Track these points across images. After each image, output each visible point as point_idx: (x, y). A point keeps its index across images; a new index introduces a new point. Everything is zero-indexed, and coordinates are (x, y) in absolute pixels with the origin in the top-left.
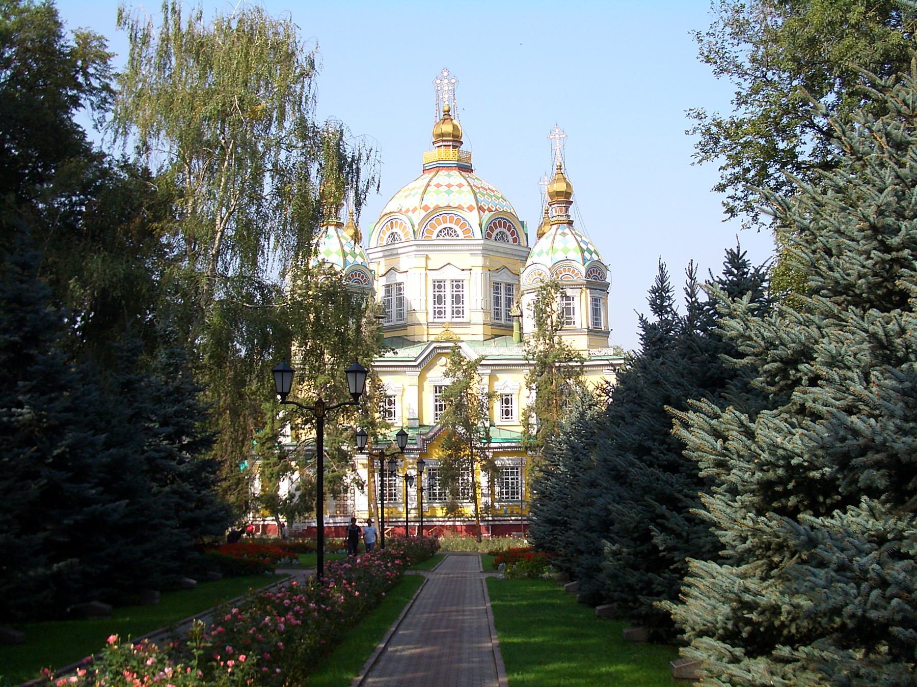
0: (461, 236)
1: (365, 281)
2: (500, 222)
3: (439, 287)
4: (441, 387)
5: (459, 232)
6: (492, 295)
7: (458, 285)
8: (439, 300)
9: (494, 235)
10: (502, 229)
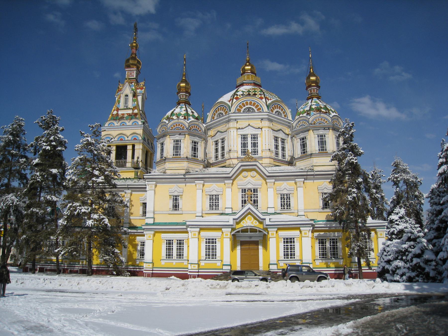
0: (256, 111)
1: (200, 131)
4: (245, 190)
5: (256, 110)
6: (274, 143)
7: (254, 137)
8: (244, 145)
9: (274, 112)
10: (278, 110)
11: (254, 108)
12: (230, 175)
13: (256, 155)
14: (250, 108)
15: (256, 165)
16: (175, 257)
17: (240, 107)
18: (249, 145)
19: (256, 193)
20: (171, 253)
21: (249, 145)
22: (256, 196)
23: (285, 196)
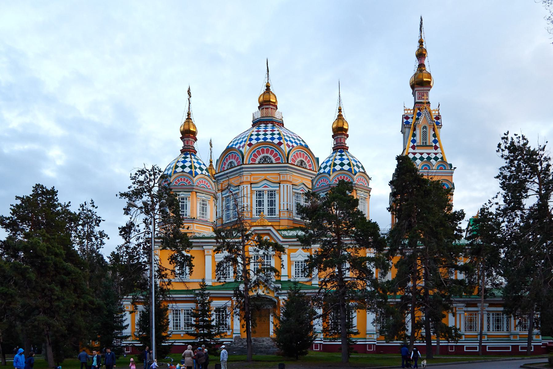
2: (300, 153)
5: (273, 160)
6: (294, 201)
7: (272, 194)
8: (260, 203)
11: (271, 157)
13: (273, 215)
14: (267, 157)
15: (270, 230)
16: (182, 328)
17: (255, 155)
18: (266, 203)
19: (269, 261)
20: (179, 324)
21: (266, 203)
22: (269, 263)
23: (300, 264)
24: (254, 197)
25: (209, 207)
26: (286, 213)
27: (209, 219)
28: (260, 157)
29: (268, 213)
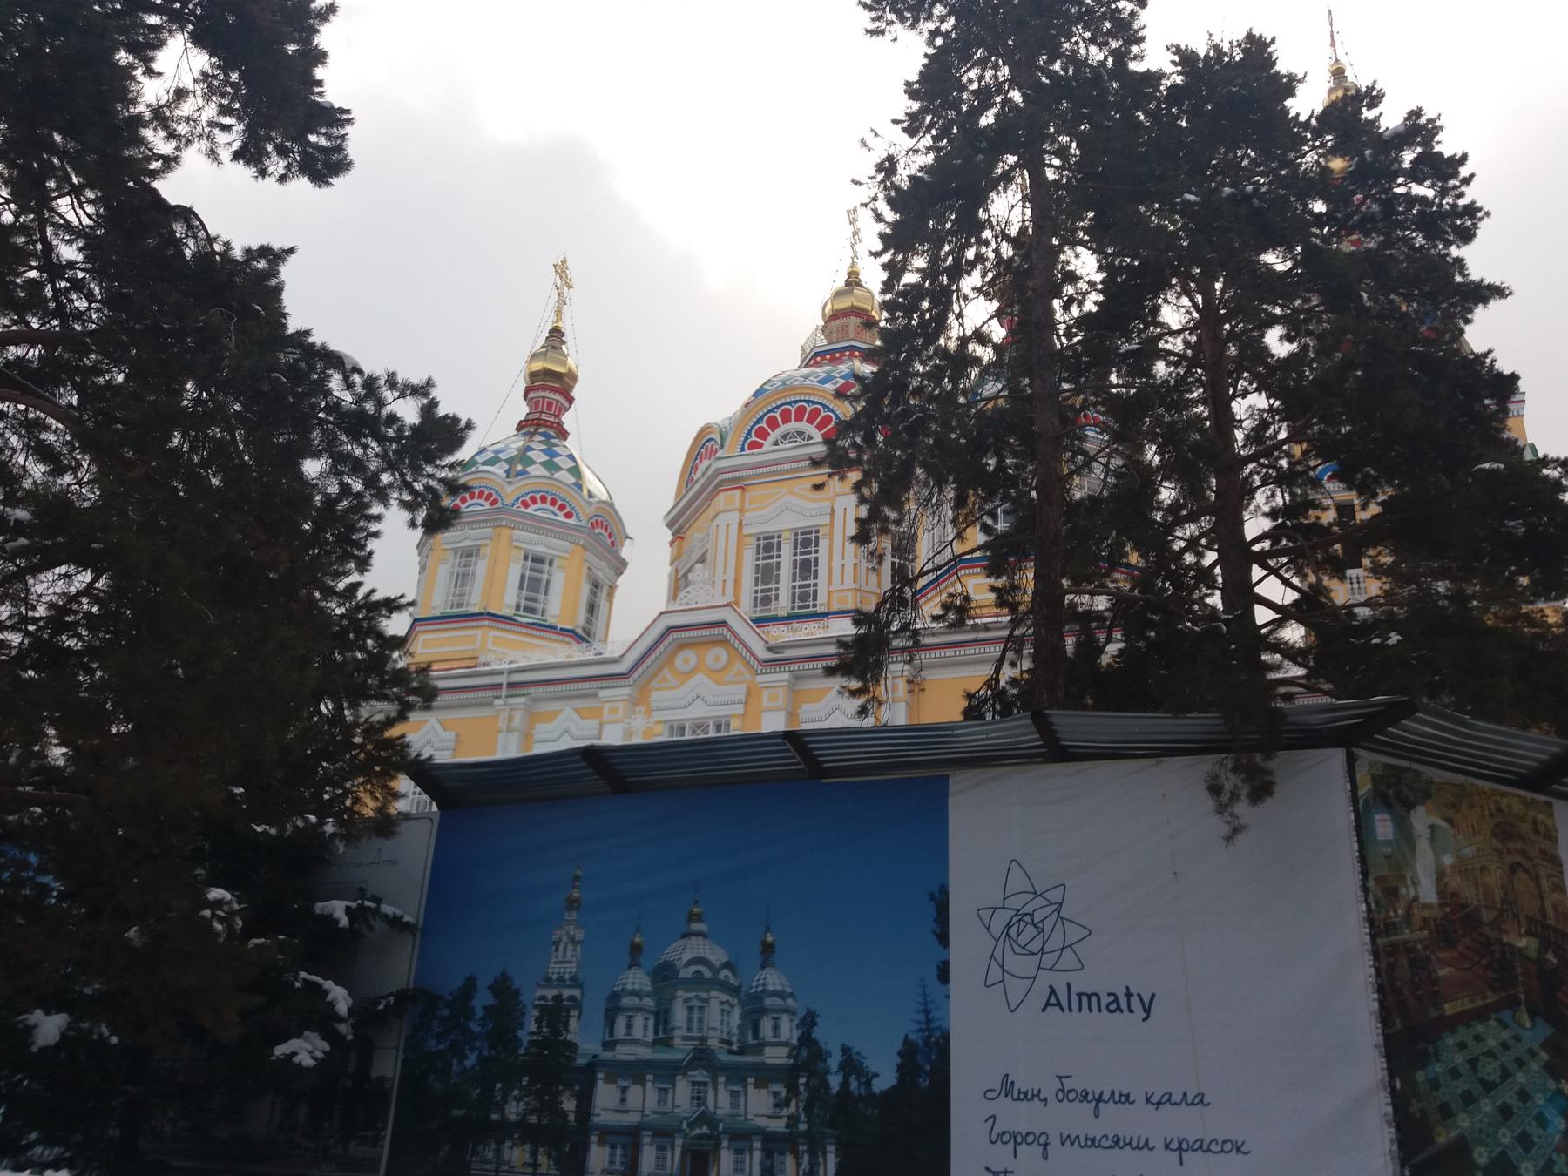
3: (768, 548)
7: (807, 541)
8: (767, 574)
12: (622, 668)
15: (723, 624)
24: (749, 557)
25: (558, 581)
26: (850, 595)
27: (554, 617)
28: (774, 435)
29: (794, 602)
